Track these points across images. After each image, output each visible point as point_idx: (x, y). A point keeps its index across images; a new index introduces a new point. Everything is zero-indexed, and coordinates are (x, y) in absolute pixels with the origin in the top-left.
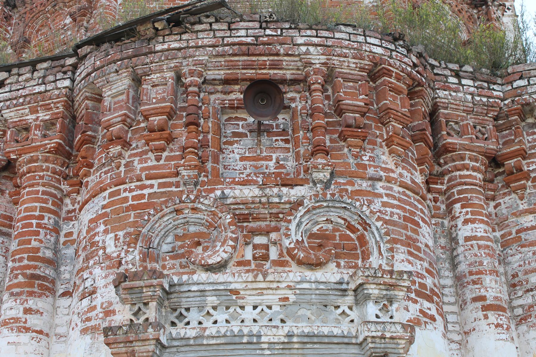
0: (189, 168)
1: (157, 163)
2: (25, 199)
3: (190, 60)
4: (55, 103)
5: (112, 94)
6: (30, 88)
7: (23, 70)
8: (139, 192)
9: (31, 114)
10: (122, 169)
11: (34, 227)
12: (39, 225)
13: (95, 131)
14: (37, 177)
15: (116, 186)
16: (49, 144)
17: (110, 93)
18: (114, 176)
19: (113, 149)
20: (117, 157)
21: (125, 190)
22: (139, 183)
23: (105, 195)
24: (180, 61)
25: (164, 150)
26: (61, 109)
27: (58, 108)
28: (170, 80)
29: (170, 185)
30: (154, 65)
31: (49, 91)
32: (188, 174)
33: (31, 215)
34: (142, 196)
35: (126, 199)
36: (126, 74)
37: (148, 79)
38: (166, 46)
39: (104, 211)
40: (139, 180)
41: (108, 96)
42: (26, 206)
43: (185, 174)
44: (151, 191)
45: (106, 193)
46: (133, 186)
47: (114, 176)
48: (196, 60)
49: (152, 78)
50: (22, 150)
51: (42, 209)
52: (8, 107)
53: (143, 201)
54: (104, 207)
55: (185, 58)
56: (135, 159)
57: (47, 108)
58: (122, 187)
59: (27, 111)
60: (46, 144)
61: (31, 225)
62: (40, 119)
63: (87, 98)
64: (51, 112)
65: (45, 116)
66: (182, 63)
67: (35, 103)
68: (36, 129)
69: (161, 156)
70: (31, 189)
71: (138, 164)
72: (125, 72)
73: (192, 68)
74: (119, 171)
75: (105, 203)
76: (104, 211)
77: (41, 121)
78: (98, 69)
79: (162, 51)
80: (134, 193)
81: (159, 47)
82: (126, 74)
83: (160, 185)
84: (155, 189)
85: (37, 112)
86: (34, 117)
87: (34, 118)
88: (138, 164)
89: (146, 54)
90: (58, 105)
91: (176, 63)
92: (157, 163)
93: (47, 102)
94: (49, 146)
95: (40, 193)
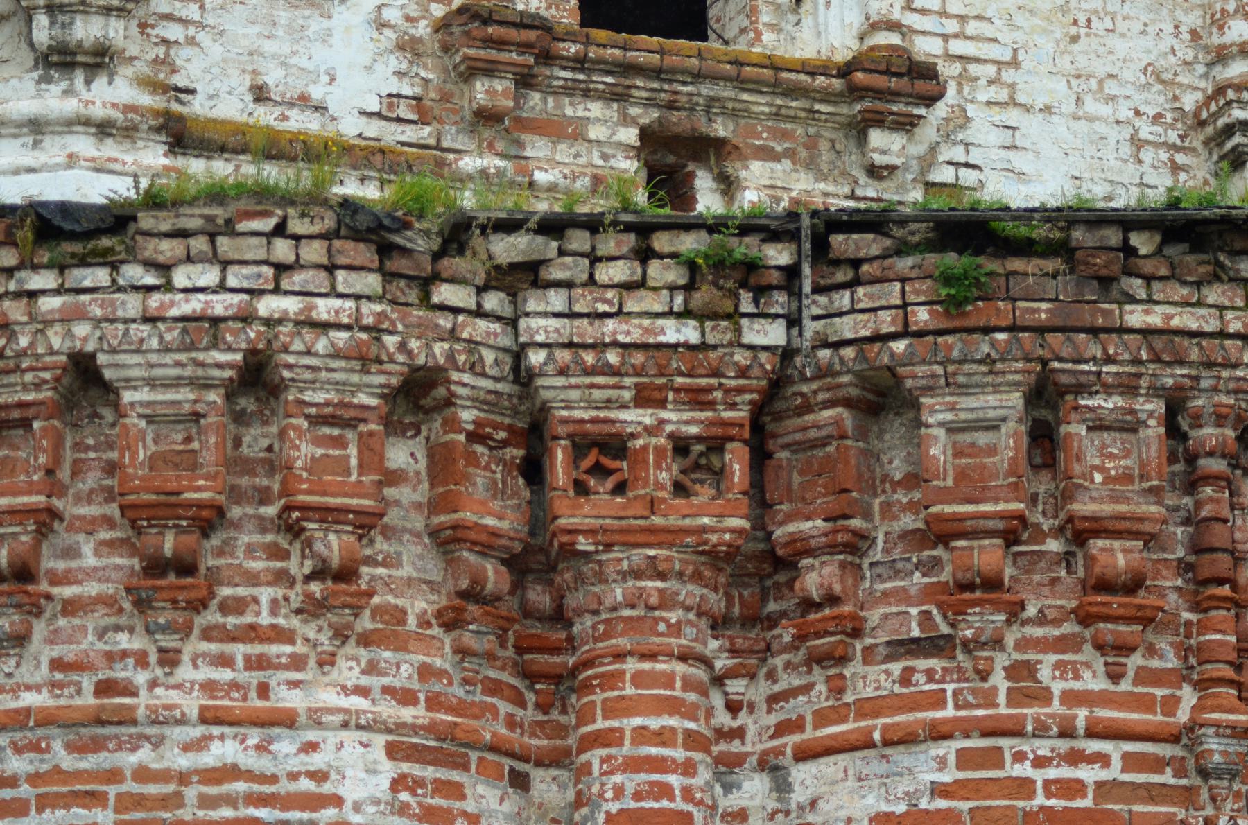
0: (1228, 731)
1: (1112, 688)
2: (623, 697)
3: (1225, 374)
4: (728, 391)
5: (952, 422)
6: (646, 322)
7: (609, 244)
8: (1066, 772)
9: (637, 406)
10: (999, 681)
11: (678, 799)
12: (687, 793)
13: (867, 515)
14: (662, 627)
15: (985, 734)
16: (713, 530)
17: (949, 416)
18: (970, 698)
19: (977, 618)
20: (985, 644)
21: (1019, 757)
22: (1063, 745)
23: (941, 752)
24: (1194, 373)
25: (1130, 650)
26: (742, 414)
27: (733, 406)
28: (1152, 422)
29: (1157, 764)
30: (1113, 368)
31: (715, 347)
32: (1222, 748)
33: (664, 759)
34: (1073, 788)
35: (1024, 787)
36: (1018, 377)
37: (1087, 407)
38: (1155, 319)
39: (942, 804)
40: (1067, 733)
41: (941, 424)
42: (638, 721)
43: (1214, 747)
44: (1104, 775)
45: (949, 749)
46: (1044, 748)
47: (970, 698)
48: (1240, 379)
49: (1100, 407)
50: (623, 531)
51: (693, 740)
52: (562, 372)
53: (1079, 803)
54: (939, 790)
55: (1210, 365)
56: (1040, 657)
57: (697, 399)
58: (1004, 742)
59: (627, 395)
60: (704, 529)
61: (665, 791)
62: (669, 428)
63: (848, 403)
64: (709, 414)
65: (688, 422)
66: (1197, 379)
67: (662, 375)
68: (658, 466)
69: (1125, 665)
70: (646, 666)
71: (1054, 678)
72: (1016, 372)
73: (1223, 399)
74: (986, 685)
75: (946, 778)
76: (942, 804)
77: (671, 436)
78: (920, 334)
79: (1147, 332)
80: (1052, 773)
81: (1136, 317)
82: (1018, 377)
83: (1131, 763)
84: (1115, 772)
85: (662, 404)
86: (646, 417)
87: (648, 421)
88: (1054, 678)
89: (1094, 331)
90: (738, 399)
91: (1183, 376)
92: (1112, 688)
93: (703, 381)
94: (714, 538)
95: (678, 684)
